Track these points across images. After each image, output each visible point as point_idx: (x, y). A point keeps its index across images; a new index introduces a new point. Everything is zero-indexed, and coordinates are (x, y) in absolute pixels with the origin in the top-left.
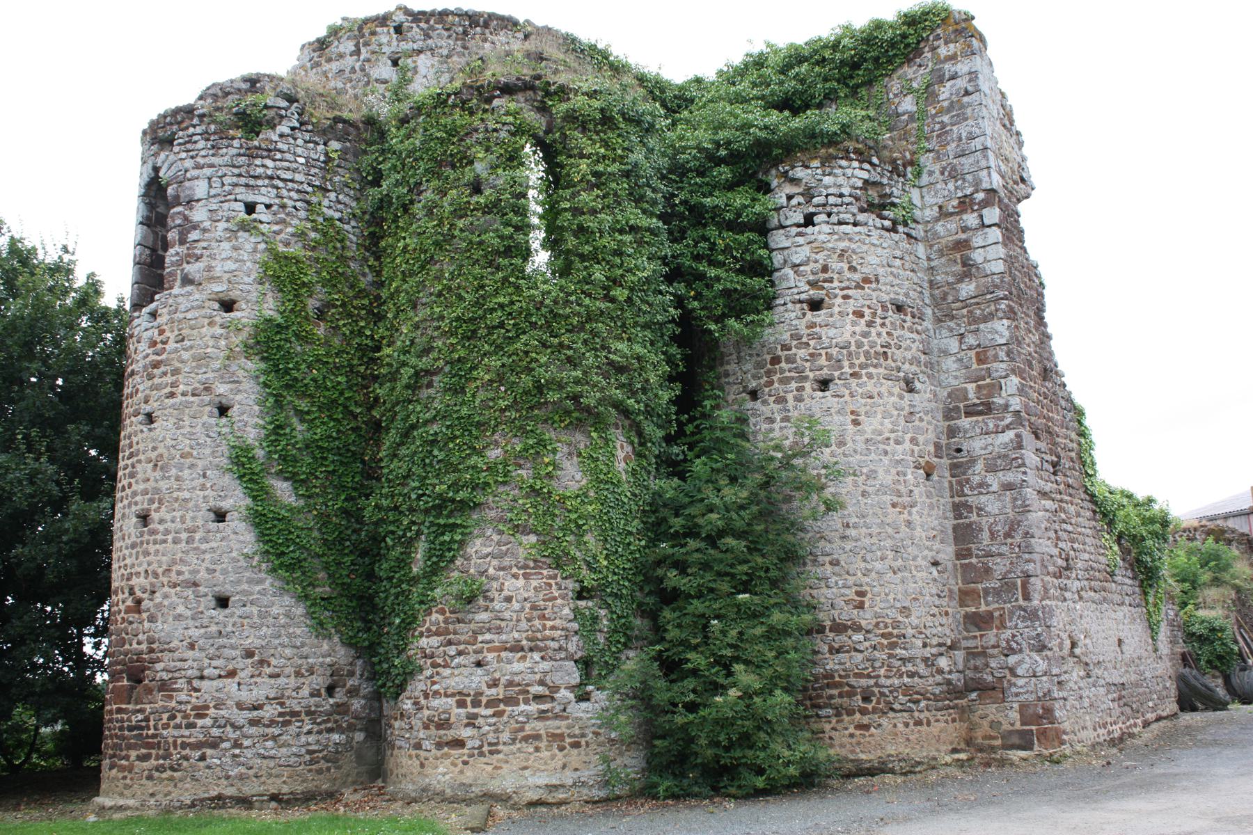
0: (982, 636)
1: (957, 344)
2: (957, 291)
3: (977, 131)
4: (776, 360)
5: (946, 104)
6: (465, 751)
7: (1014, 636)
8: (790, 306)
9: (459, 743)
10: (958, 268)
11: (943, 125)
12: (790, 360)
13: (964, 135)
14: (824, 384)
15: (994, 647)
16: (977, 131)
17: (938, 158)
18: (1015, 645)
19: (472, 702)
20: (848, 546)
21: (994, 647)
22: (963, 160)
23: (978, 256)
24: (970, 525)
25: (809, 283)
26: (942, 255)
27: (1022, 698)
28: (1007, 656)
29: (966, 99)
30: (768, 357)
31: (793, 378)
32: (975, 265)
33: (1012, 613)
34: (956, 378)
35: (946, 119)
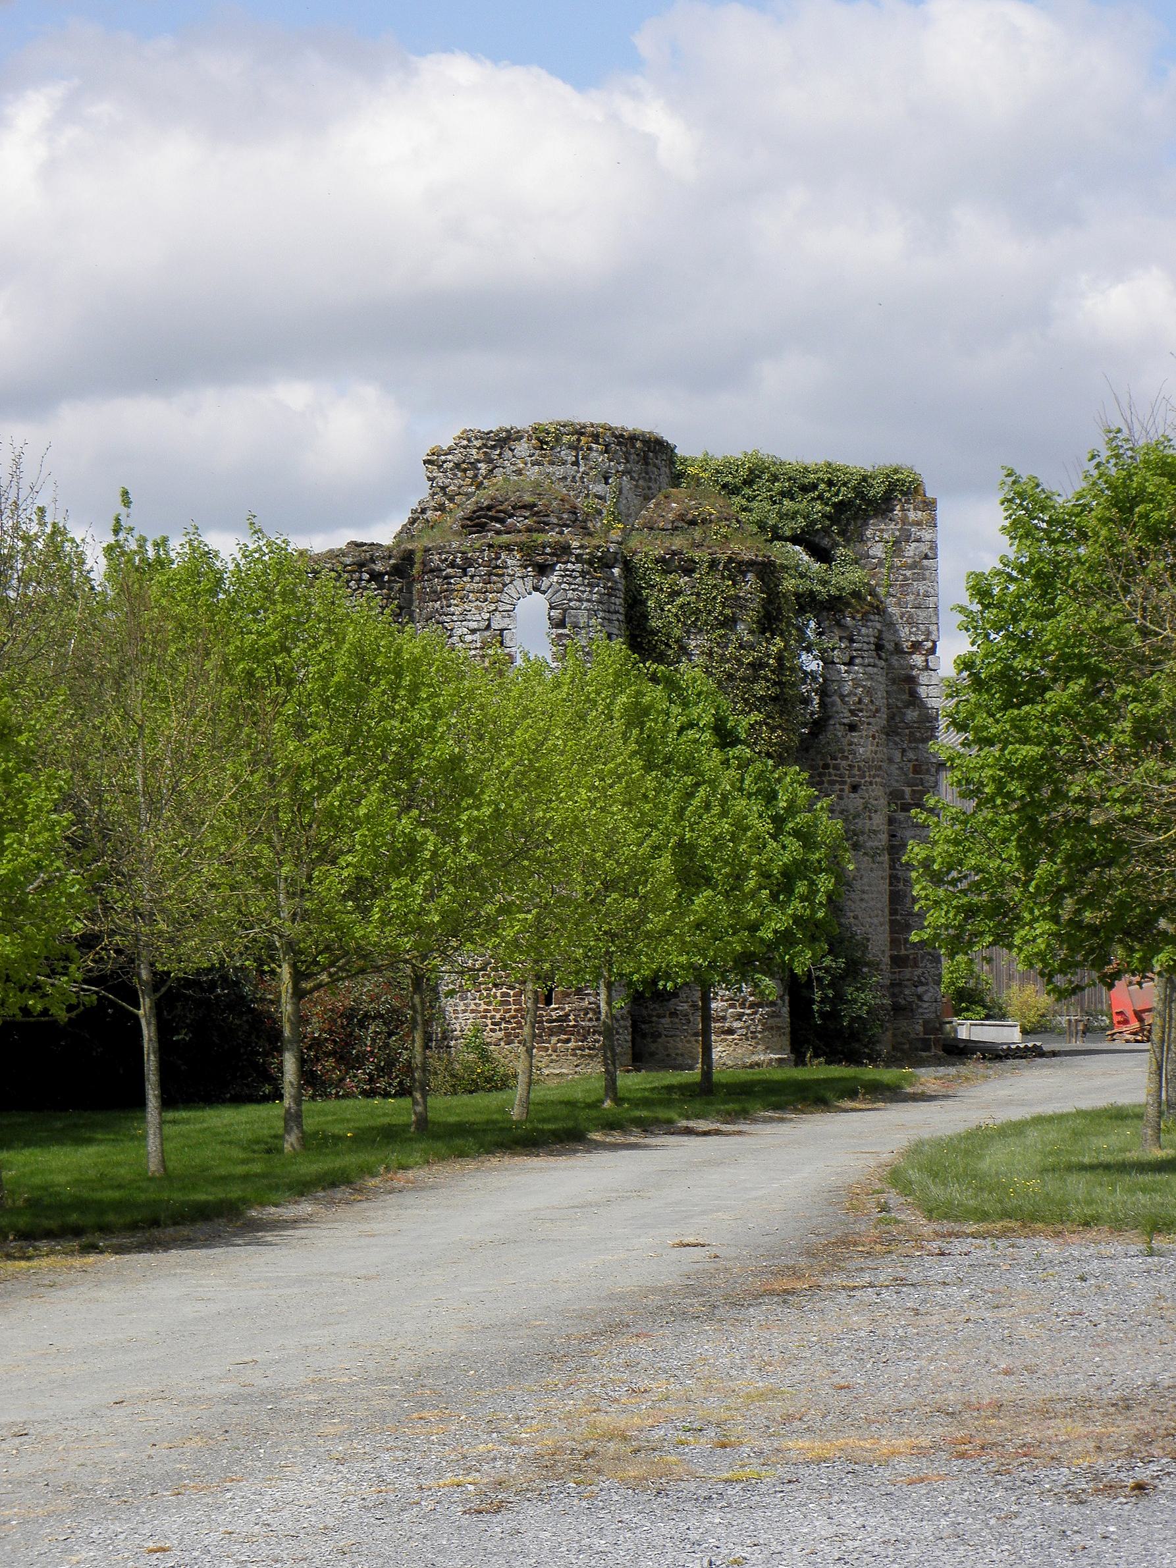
0: (899, 972)
1: (900, 755)
2: (904, 714)
3: (932, 591)
4: (826, 766)
5: (909, 561)
6: (735, 1036)
7: (923, 973)
8: (837, 726)
9: (731, 1031)
10: (906, 697)
11: (906, 578)
12: (836, 768)
13: (922, 592)
14: (855, 788)
15: (908, 980)
16: (932, 591)
17: (899, 604)
18: (923, 979)
19: (740, 1005)
20: (864, 905)
21: (908, 980)
22: (919, 612)
23: (923, 691)
24: (899, 891)
25: (851, 711)
26: (894, 683)
27: (926, 1016)
28: (916, 987)
29: (925, 562)
30: (821, 763)
31: (837, 781)
32: (920, 699)
33: (923, 957)
34: (897, 781)
35: (908, 573)
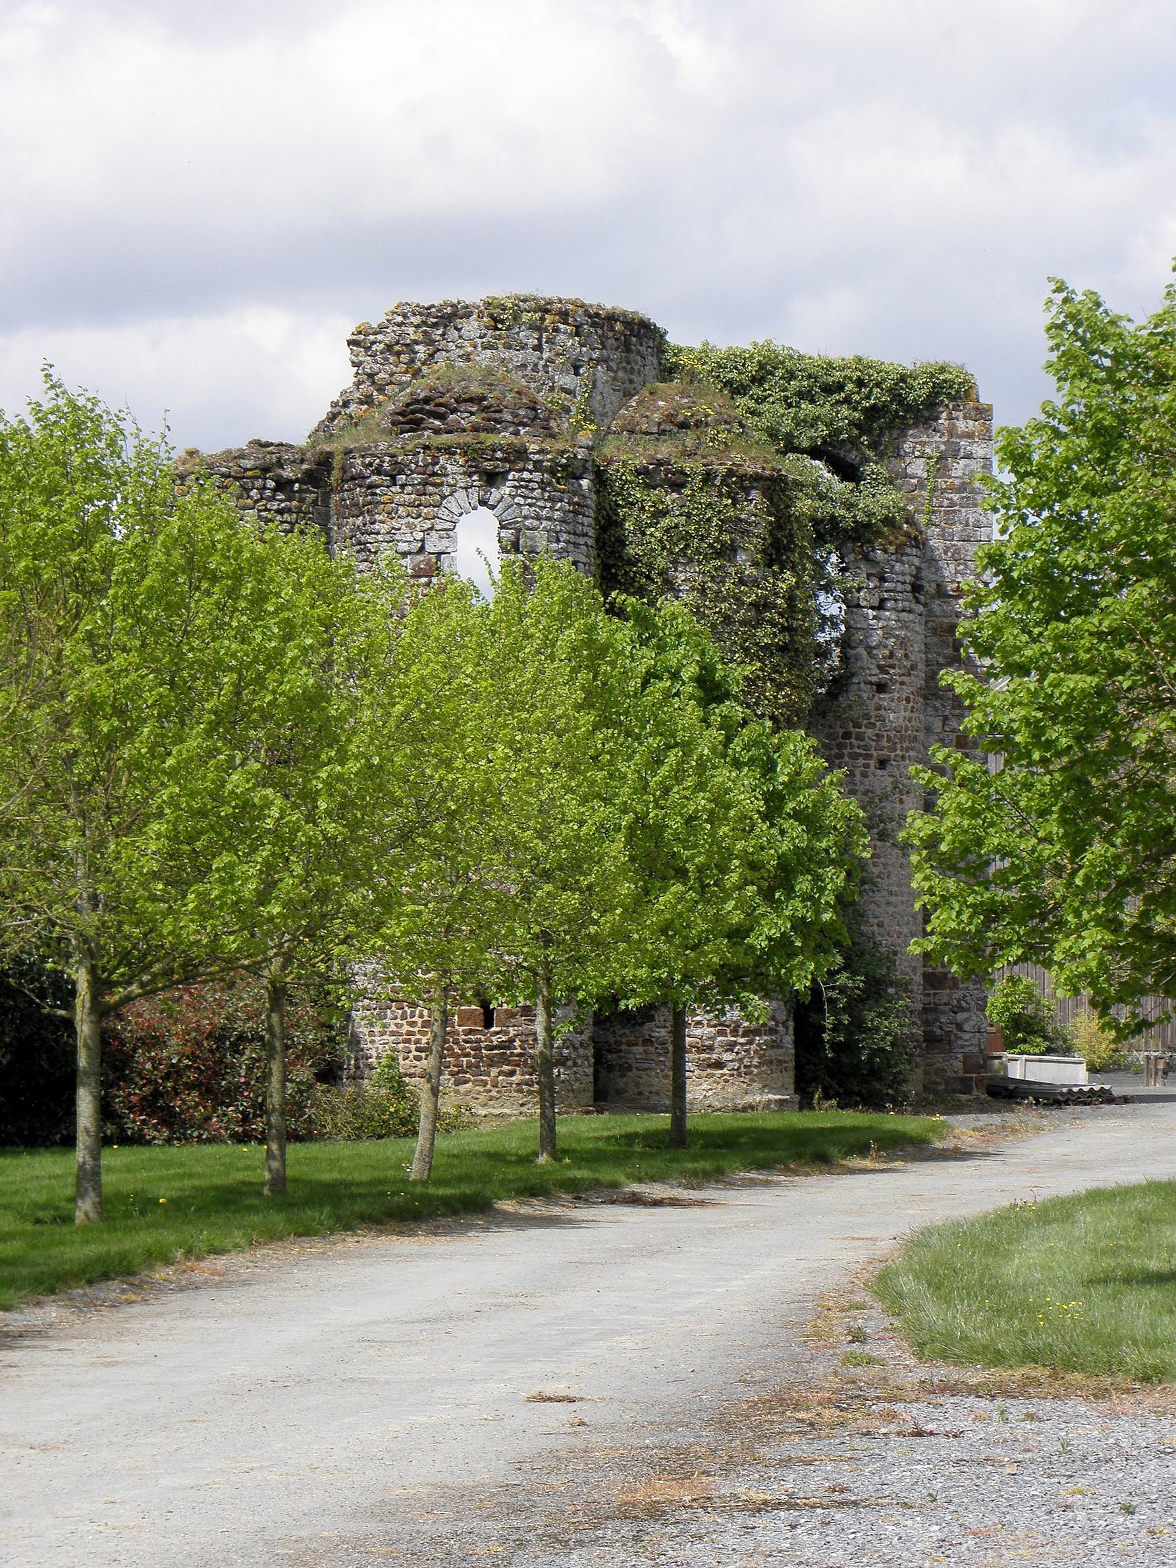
0: (935, 994)
4: (847, 735)
6: (725, 1071)
9: (719, 1065)
11: (952, 504)
12: (860, 737)
13: (971, 521)
14: (883, 764)
15: (945, 1004)
17: (943, 536)
18: (964, 1004)
20: (891, 910)
21: (945, 1004)
25: (879, 667)
26: (935, 634)
27: (967, 1050)
28: (955, 1013)
30: (841, 731)
31: (861, 755)
35: (956, 497)
